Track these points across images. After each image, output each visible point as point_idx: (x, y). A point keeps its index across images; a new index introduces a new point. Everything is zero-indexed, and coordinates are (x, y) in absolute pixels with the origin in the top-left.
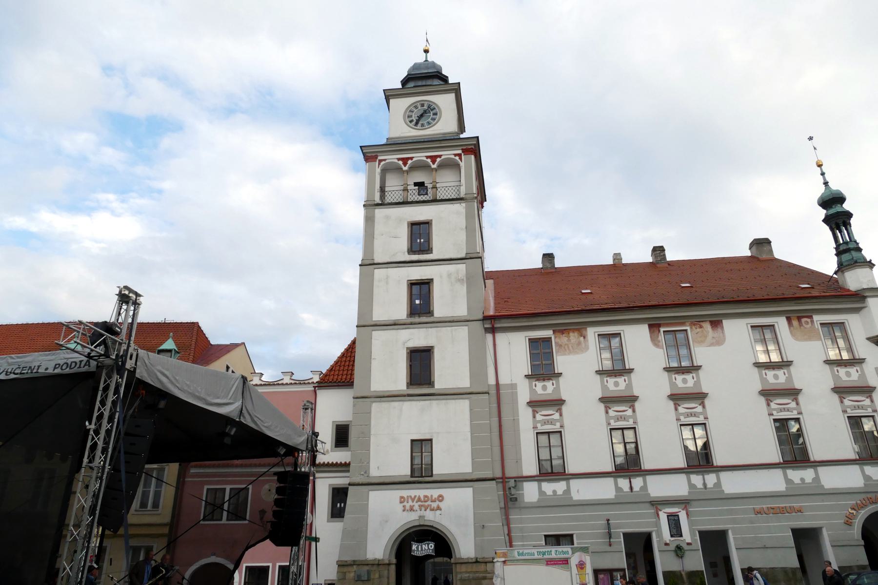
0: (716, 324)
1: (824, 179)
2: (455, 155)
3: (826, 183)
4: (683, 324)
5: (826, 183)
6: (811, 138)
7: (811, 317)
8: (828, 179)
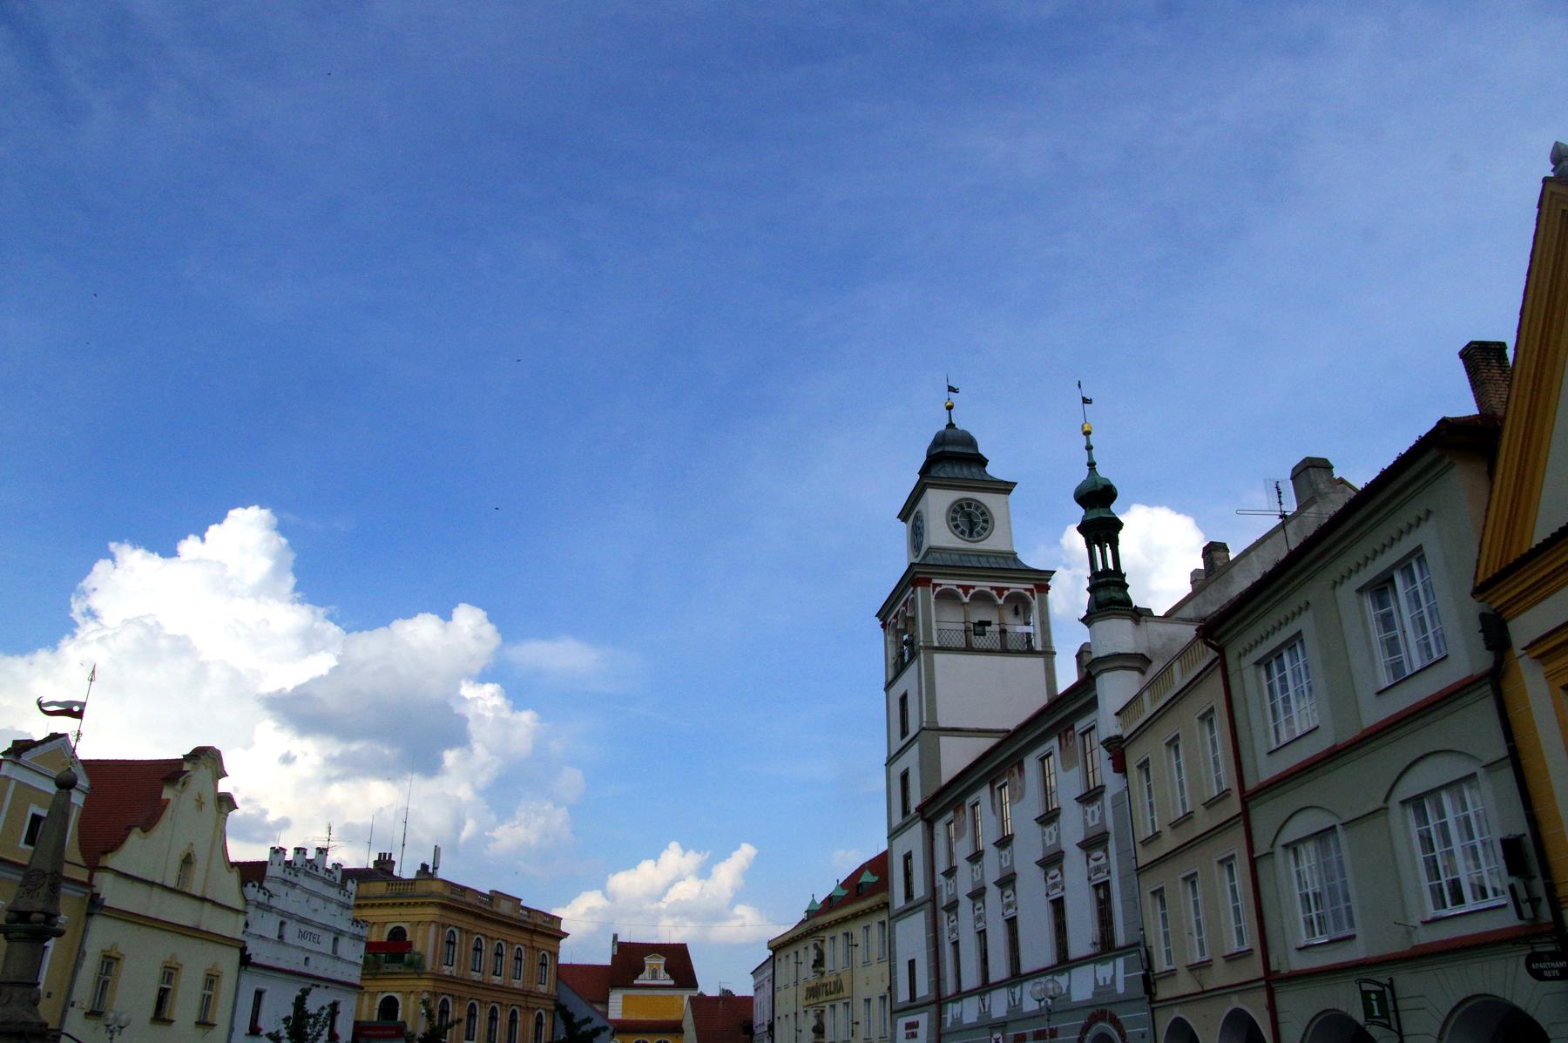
1: (1090, 456)
3: (1092, 465)
4: (1003, 776)
5: (1092, 465)
7: (1072, 728)
8: (1096, 459)
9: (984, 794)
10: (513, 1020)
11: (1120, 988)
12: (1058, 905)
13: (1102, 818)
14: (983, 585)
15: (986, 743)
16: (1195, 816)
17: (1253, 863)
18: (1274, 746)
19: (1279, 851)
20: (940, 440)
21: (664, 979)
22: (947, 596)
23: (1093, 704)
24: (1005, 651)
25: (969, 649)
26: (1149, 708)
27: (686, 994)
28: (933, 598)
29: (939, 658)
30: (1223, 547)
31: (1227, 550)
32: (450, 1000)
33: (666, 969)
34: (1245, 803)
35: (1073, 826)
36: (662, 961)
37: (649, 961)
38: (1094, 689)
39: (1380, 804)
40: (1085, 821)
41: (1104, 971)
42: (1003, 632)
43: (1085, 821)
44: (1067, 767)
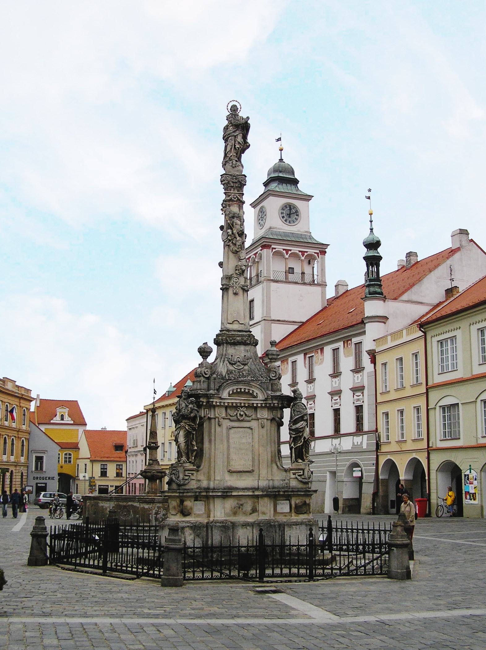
0: (322, 350)
2: (261, 250)
3: (372, 229)
4: (312, 352)
5: (372, 229)
6: (370, 190)
7: (351, 340)
8: (373, 227)
9: (300, 358)
10: (13, 444)
11: (365, 446)
12: (337, 412)
13: (362, 379)
14: (295, 250)
15: (292, 328)
16: (406, 388)
17: (428, 410)
18: (440, 372)
19: (438, 408)
20: (276, 169)
21: (67, 420)
22: (278, 254)
23: (364, 333)
24: (305, 284)
25: (287, 282)
26: (390, 344)
27: (81, 429)
28: (271, 254)
29: (273, 285)
30: (416, 254)
31: (417, 256)
32: (7, 437)
33: (69, 416)
34: (427, 389)
35: (347, 380)
36: (65, 411)
37: (59, 411)
38: (365, 328)
39: (474, 400)
40: (354, 380)
41: (358, 440)
42: (303, 273)
43: (354, 380)
44: (346, 356)
